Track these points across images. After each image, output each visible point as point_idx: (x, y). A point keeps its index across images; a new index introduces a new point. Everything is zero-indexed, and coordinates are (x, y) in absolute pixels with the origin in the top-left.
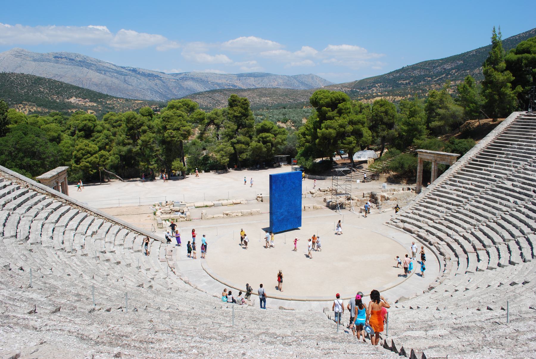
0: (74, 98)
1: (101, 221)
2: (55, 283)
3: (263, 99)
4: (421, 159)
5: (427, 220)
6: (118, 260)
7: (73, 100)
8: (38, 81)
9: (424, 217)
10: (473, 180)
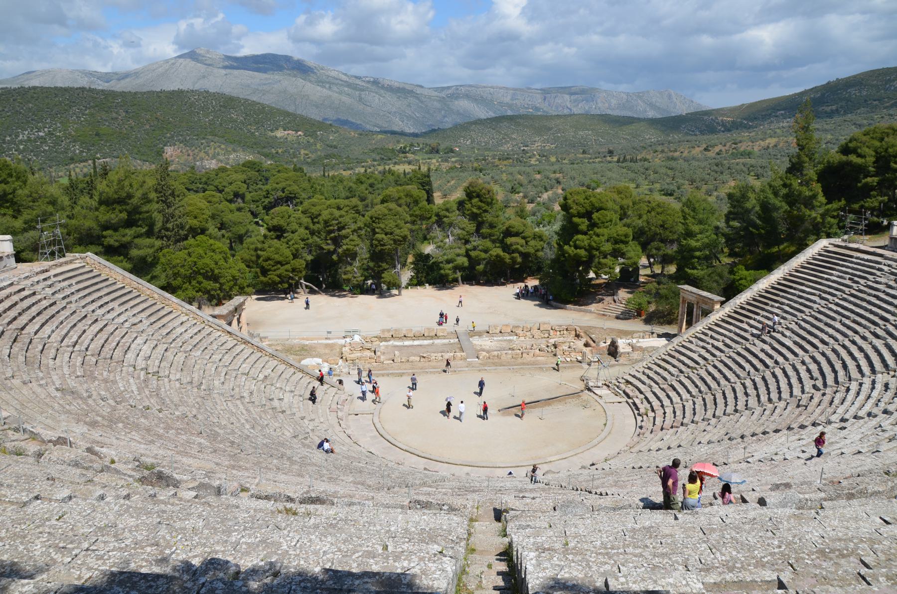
0: (281, 130)
1: (276, 362)
2: (219, 431)
3: (581, 133)
4: (683, 298)
5: (653, 384)
6: (284, 409)
7: (280, 133)
8: (228, 102)
9: (652, 379)
10: (725, 336)
